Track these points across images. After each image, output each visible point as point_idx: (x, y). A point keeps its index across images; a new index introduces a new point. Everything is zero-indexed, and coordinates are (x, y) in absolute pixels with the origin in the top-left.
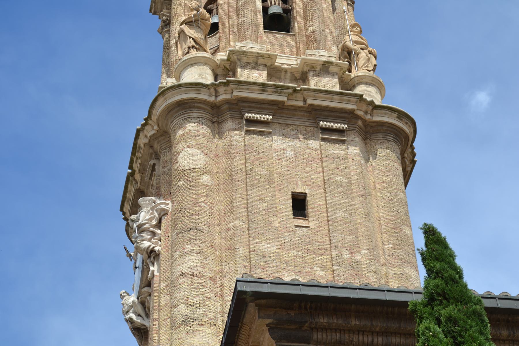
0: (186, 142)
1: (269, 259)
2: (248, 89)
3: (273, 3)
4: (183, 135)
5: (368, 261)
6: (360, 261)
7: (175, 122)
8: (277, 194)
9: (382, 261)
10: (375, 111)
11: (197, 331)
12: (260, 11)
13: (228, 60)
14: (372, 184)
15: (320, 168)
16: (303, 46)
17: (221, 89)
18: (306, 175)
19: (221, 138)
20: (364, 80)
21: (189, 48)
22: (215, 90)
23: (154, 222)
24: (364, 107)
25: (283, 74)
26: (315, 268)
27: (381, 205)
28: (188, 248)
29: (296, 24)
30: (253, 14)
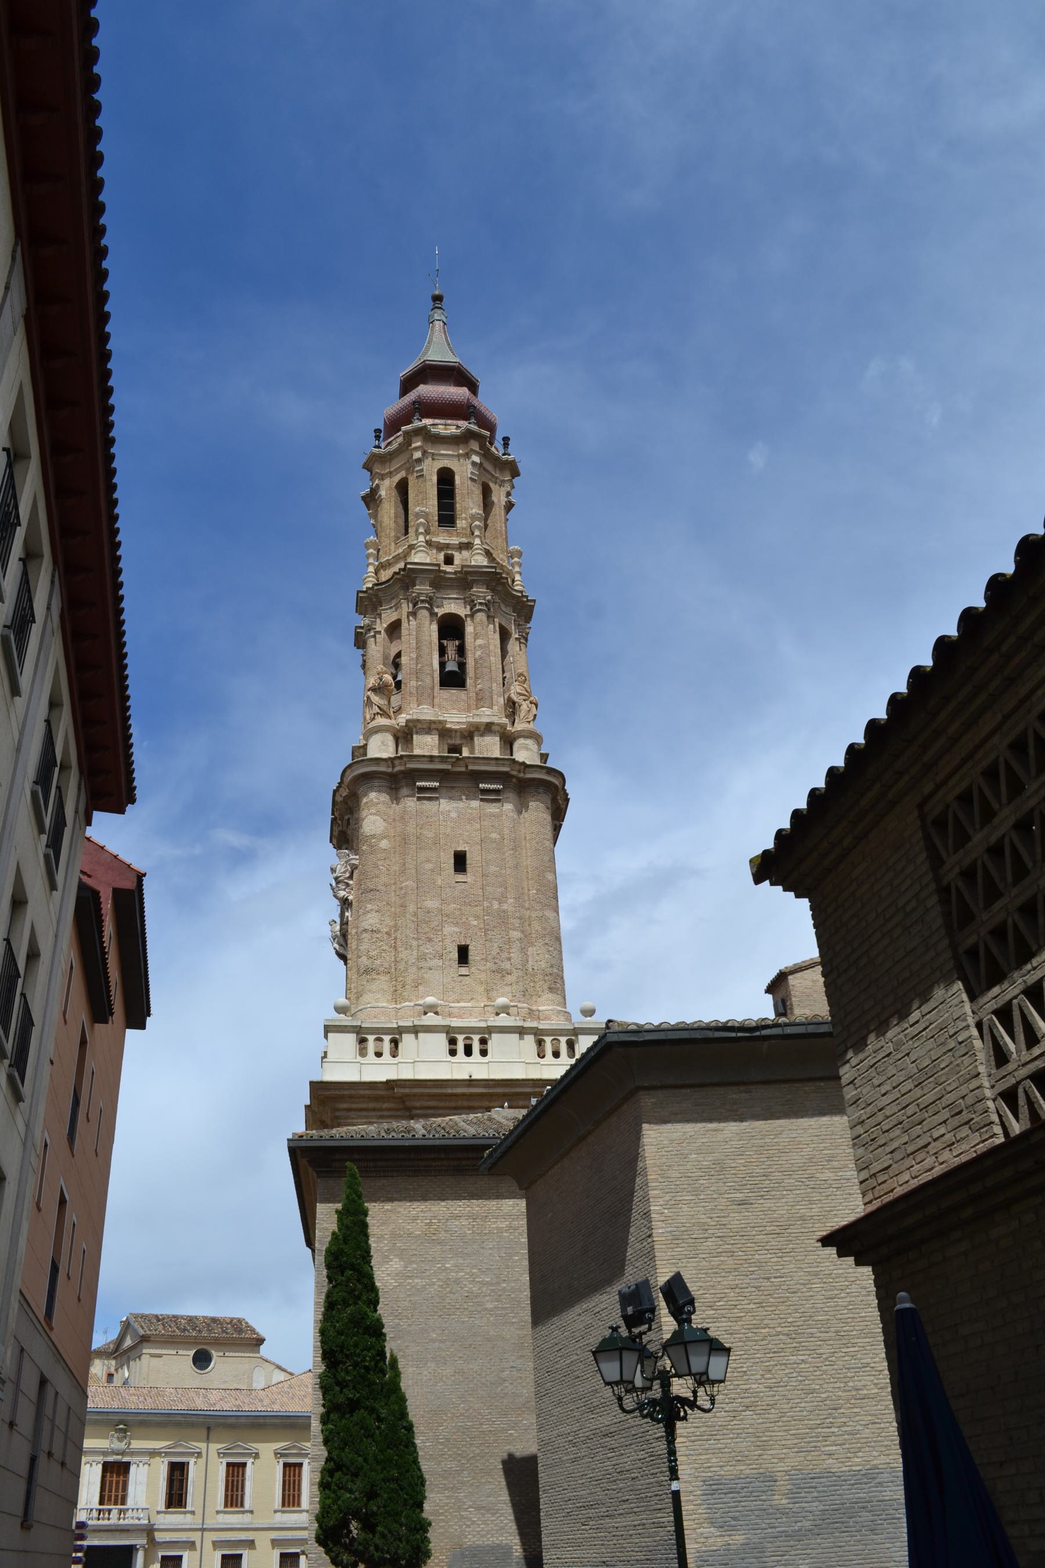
0: (369, 810)
1: (432, 914)
2: (418, 761)
3: (450, 658)
4: (367, 803)
5: (514, 909)
6: (507, 910)
7: (361, 789)
8: (442, 854)
9: (527, 905)
10: (527, 769)
11: (375, 979)
13: (406, 726)
14: (523, 835)
15: (478, 826)
16: (473, 702)
17: (397, 762)
18: (467, 834)
19: (398, 804)
20: (523, 734)
21: (374, 714)
22: (392, 762)
23: (347, 875)
24: (517, 767)
25: (454, 733)
26: (470, 919)
27: (529, 854)
28: (369, 907)
29: (468, 680)
30: (429, 677)
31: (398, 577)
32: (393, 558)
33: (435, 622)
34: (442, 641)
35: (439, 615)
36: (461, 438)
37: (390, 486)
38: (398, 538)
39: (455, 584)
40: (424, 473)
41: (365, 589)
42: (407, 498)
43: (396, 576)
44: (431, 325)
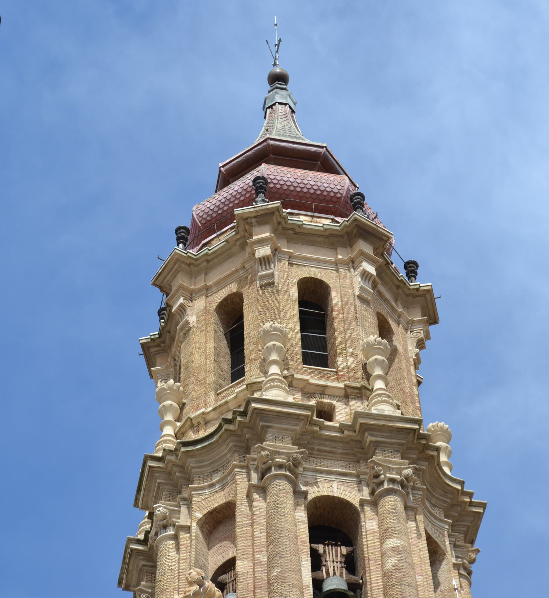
3: (331, 573)
12: (308, 586)
30: (296, 591)
31: (231, 427)
32: (214, 409)
33: (303, 507)
34: (315, 546)
35: (310, 497)
36: (342, 236)
37: (206, 308)
38: (221, 387)
39: (340, 451)
40: (276, 280)
41: (160, 454)
42: (241, 327)
43: (226, 427)
44: (268, 110)
